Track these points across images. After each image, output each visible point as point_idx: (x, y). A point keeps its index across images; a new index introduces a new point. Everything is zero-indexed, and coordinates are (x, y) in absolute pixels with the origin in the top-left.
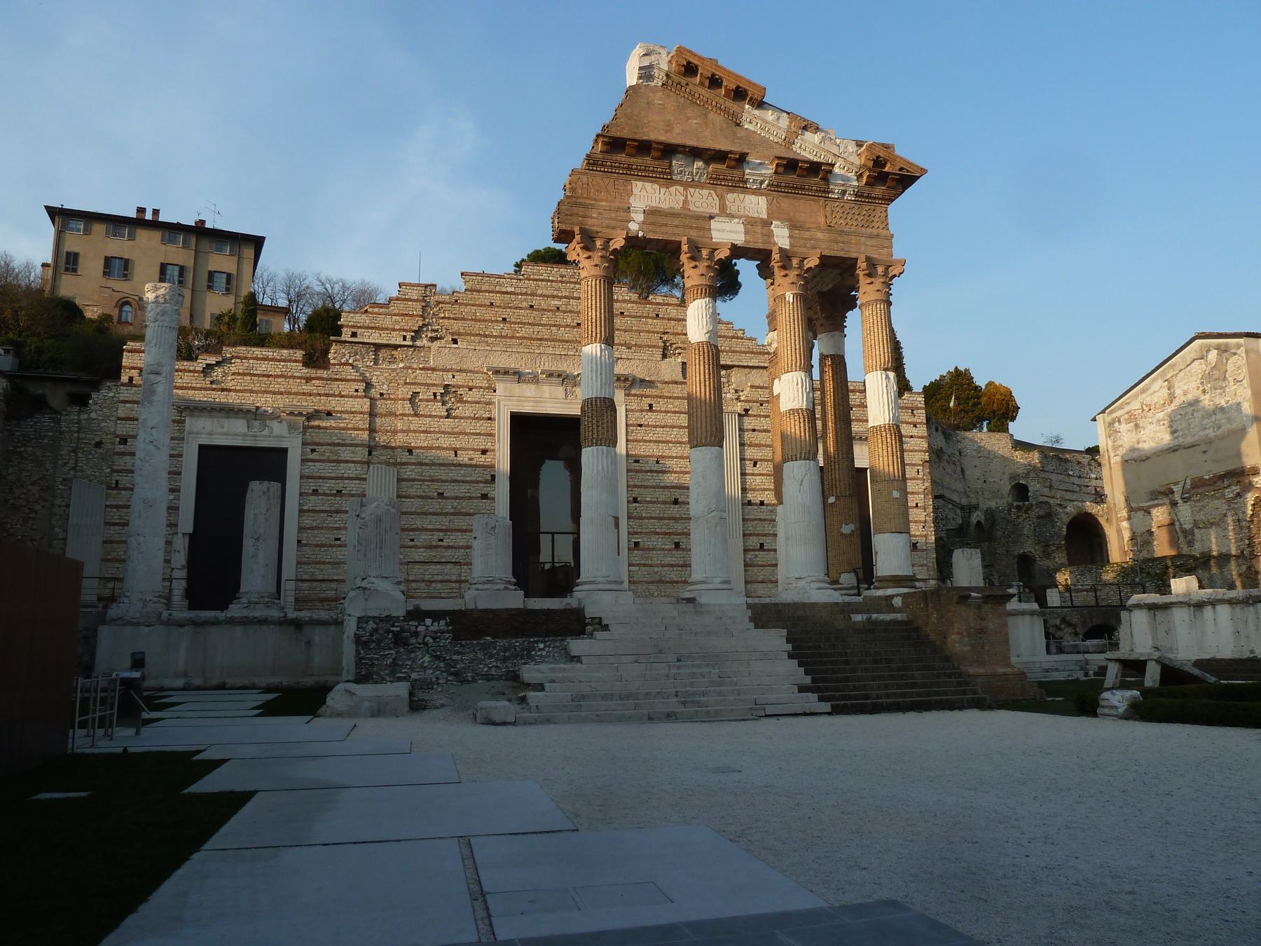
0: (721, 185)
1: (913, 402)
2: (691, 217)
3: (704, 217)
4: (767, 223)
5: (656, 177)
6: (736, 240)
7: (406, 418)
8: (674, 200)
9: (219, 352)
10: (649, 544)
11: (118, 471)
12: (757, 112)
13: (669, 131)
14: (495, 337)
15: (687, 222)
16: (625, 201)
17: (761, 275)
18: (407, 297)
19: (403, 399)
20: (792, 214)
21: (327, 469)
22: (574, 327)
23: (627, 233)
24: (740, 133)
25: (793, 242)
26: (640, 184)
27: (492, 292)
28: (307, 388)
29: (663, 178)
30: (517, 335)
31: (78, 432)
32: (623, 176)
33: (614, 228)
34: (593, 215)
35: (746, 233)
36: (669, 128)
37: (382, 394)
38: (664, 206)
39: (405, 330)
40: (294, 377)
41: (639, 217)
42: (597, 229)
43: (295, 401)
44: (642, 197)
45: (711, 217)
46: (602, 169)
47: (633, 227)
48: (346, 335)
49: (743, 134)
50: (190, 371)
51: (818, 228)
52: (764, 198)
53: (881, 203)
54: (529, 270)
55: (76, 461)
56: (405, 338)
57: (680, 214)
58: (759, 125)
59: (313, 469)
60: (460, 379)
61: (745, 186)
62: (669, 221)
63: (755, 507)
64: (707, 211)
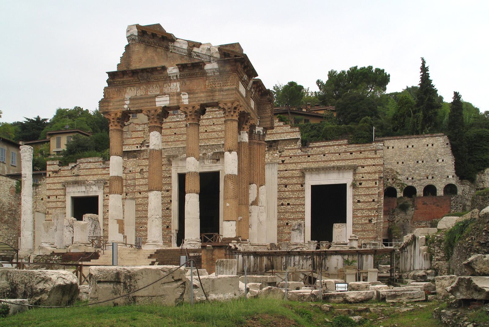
0: (160, 81)
1: (376, 147)
2: (147, 98)
3: (153, 97)
4: (179, 94)
7: (138, 180)
9: (76, 162)
11: (48, 208)
14: (172, 142)
15: (146, 100)
18: (138, 130)
19: (137, 173)
20: (191, 87)
22: (204, 133)
26: (129, 88)
27: (170, 122)
29: (137, 83)
30: (181, 139)
31: (36, 195)
33: (118, 109)
35: (170, 100)
37: (130, 171)
39: (137, 144)
40: (99, 168)
45: (156, 96)
47: (126, 106)
50: (67, 170)
52: (179, 82)
53: (232, 73)
55: (36, 206)
56: (137, 147)
57: (143, 98)
63: (285, 206)
64: (155, 93)
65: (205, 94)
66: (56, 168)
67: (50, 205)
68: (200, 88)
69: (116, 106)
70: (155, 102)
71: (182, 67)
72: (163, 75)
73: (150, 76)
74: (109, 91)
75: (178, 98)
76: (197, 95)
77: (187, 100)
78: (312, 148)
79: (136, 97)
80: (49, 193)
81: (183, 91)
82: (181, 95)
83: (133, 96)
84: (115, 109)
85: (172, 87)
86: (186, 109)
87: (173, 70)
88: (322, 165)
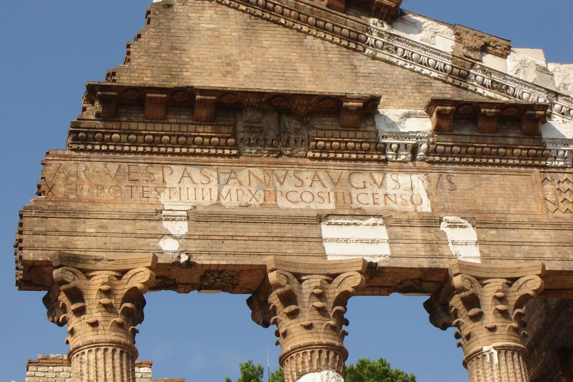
0: (335, 159)
4: (431, 222)
5: (209, 155)
6: (373, 256)
8: (247, 192)
13: (228, 72)
15: (275, 229)
16: (152, 200)
17: (434, 320)
20: (480, 201)
23: (155, 258)
25: (486, 251)
26: (178, 170)
29: (222, 155)
32: (147, 156)
33: (129, 251)
34: (88, 230)
35: (392, 241)
36: (229, 69)
41: (181, 228)
42: (96, 254)
44: (184, 192)
45: (321, 218)
46: (104, 148)
47: (169, 247)
52: (422, 175)
54: (38, 374)
57: (259, 217)
58: (400, 50)
61: (383, 157)
62: (240, 229)
64: (313, 206)
65: (552, 233)
68: (520, 208)
69: (117, 240)
70: (320, 239)
72: (359, 135)
73: (297, 131)
74: (73, 169)
75: (430, 236)
76: (513, 232)
79: (217, 210)
81: (446, 211)
82: (443, 226)
83: (205, 207)
84: (108, 250)
85: (390, 191)
86: (477, 284)
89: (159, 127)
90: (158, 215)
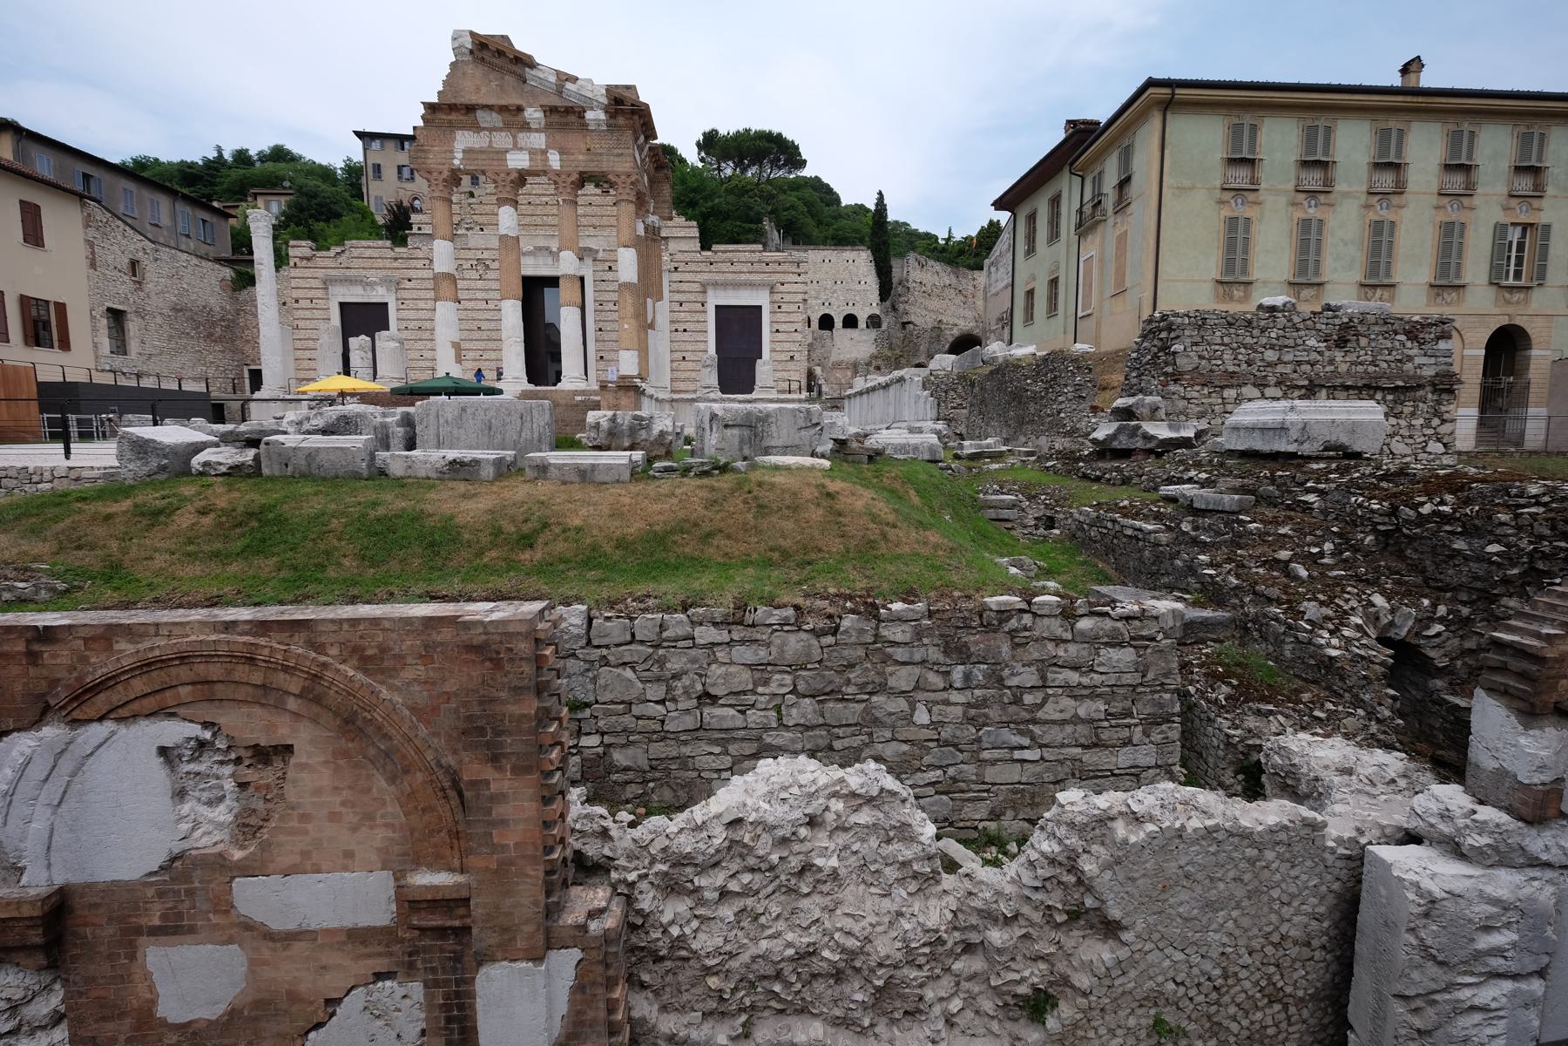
4: (544, 152)
10: (609, 357)
12: (534, 72)
21: (412, 315)
24: (527, 88)
28: (395, 265)
38: (476, 146)
41: (460, 155)
43: (390, 273)
45: (507, 151)
47: (456, 162)
48: (415, 227)
49: (529, 88)
51: (581, 153)
59: (404, 314)
60: (486, 255)
62: (479, 156)
66: (307, 252)
67: (301, 314)
71: (550, 111)
77: (558, 164)
78: (716, 252)
80: (295, 294)
87: (533, 114)
88: (730, 277)
89: (450, 117)
90: (452, 152)
